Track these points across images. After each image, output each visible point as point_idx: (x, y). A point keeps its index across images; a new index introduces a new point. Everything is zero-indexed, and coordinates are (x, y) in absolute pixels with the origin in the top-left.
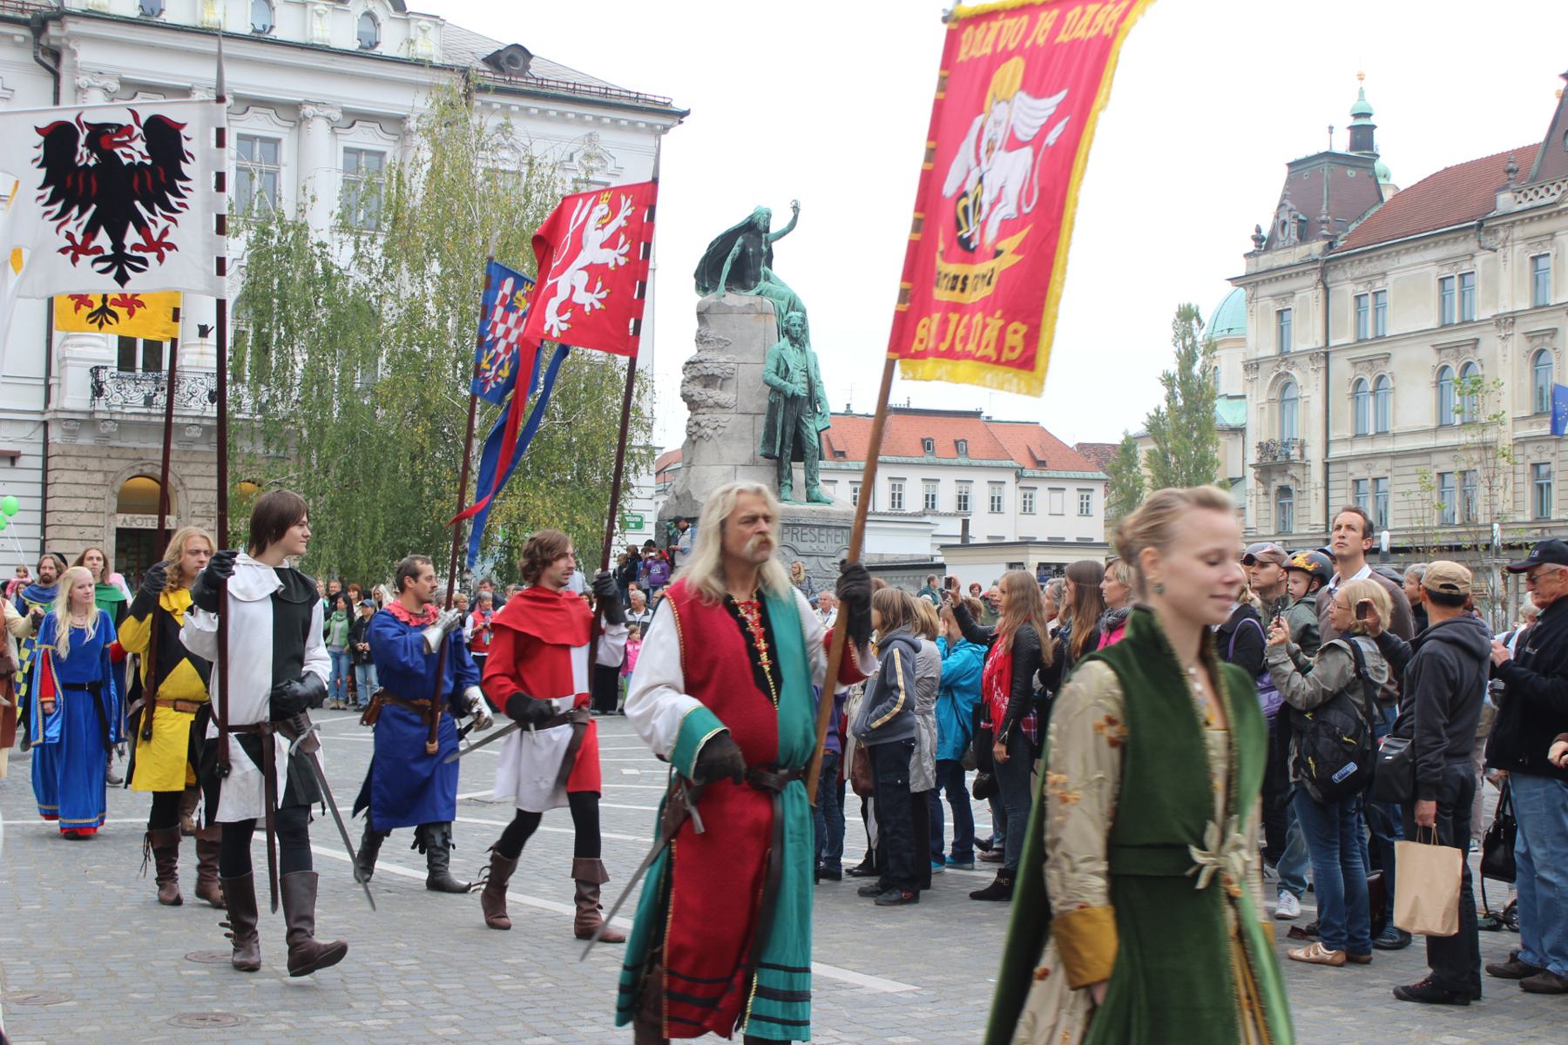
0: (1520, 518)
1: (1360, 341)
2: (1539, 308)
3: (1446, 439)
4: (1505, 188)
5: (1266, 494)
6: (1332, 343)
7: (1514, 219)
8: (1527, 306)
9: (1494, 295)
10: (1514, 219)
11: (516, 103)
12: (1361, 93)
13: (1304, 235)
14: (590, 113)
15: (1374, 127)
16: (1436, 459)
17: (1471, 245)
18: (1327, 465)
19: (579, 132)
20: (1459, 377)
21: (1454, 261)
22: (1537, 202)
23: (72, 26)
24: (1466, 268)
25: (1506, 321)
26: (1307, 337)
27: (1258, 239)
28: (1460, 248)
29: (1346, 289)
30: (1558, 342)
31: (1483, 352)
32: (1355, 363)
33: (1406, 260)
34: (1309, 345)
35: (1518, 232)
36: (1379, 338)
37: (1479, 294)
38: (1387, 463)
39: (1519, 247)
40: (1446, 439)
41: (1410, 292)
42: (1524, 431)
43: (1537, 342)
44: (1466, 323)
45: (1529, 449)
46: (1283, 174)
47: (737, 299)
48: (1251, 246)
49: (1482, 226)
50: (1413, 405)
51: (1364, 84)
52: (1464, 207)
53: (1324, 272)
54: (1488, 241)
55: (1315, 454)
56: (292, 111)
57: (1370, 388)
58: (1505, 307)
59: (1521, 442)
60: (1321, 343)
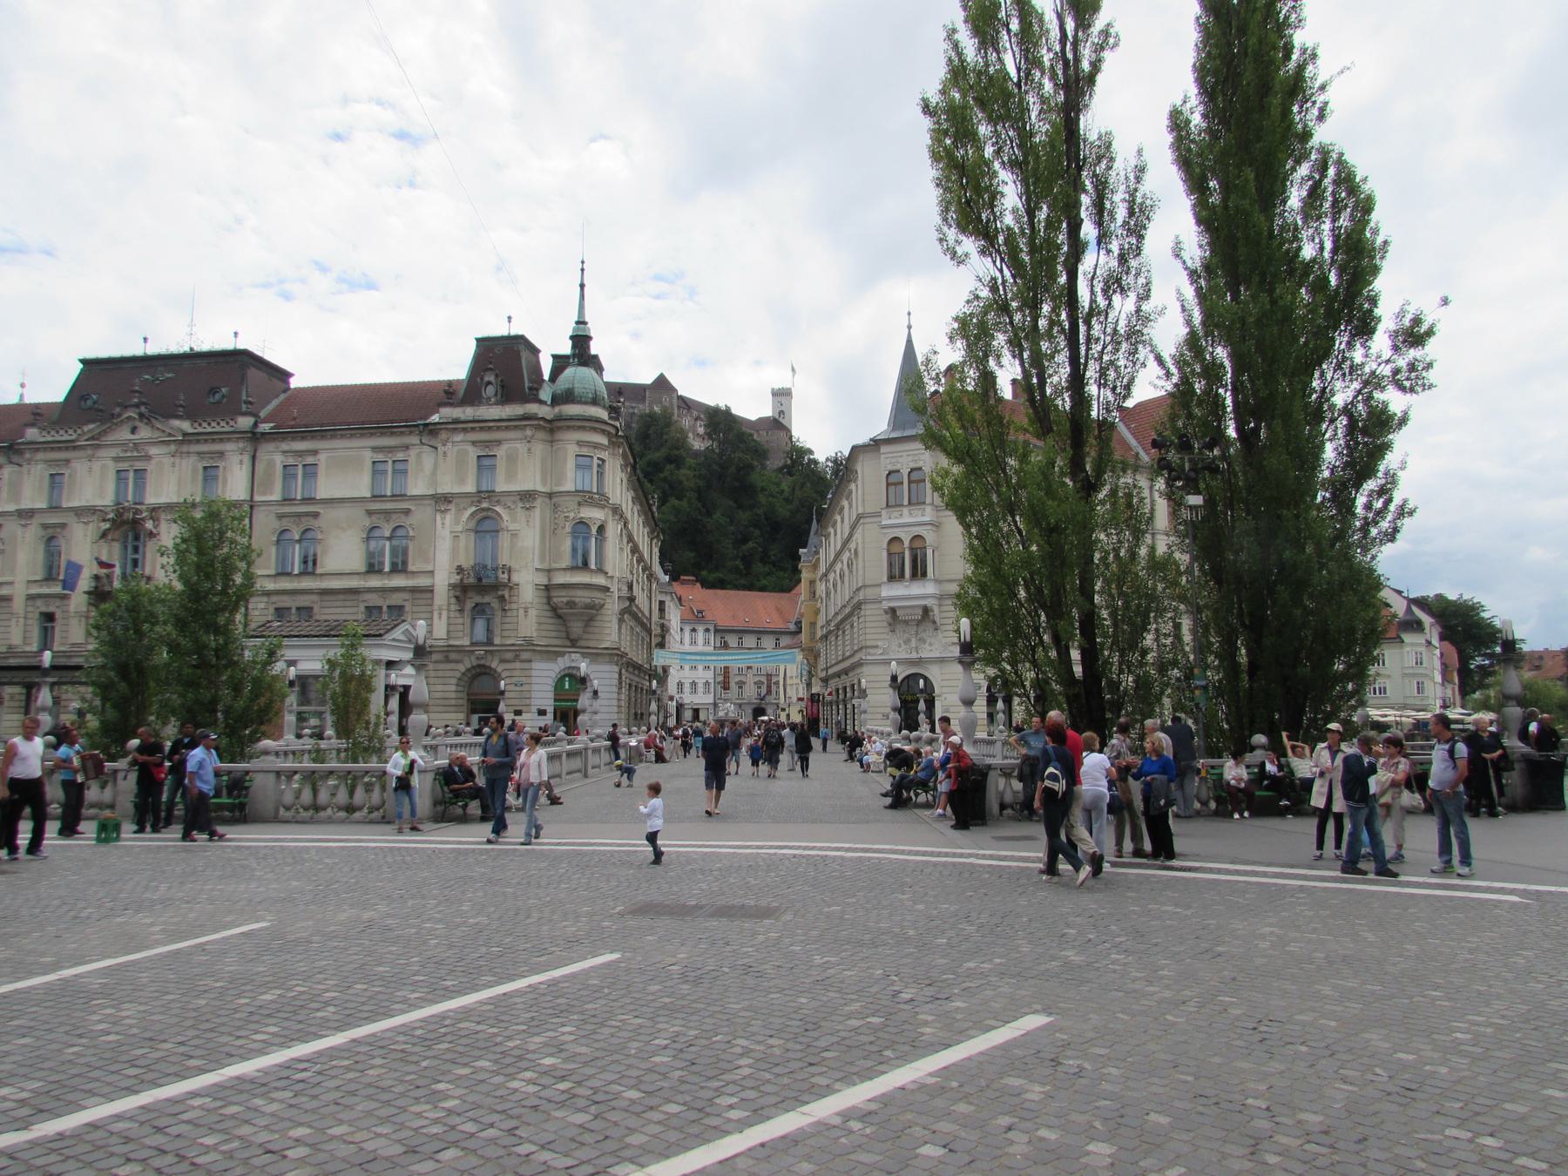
0: (28, 649)
2: (54, 508)
4: (32, 425)
7: (36, 446)
8: (42, 504)
10: (36, 446)
35: (40, 456)
39: (40, 467)
42: (35, 590)
43: (50, 531)
45: (39, 603)
54: (16, 459)
58: (26, 504)
59: (31, 598)
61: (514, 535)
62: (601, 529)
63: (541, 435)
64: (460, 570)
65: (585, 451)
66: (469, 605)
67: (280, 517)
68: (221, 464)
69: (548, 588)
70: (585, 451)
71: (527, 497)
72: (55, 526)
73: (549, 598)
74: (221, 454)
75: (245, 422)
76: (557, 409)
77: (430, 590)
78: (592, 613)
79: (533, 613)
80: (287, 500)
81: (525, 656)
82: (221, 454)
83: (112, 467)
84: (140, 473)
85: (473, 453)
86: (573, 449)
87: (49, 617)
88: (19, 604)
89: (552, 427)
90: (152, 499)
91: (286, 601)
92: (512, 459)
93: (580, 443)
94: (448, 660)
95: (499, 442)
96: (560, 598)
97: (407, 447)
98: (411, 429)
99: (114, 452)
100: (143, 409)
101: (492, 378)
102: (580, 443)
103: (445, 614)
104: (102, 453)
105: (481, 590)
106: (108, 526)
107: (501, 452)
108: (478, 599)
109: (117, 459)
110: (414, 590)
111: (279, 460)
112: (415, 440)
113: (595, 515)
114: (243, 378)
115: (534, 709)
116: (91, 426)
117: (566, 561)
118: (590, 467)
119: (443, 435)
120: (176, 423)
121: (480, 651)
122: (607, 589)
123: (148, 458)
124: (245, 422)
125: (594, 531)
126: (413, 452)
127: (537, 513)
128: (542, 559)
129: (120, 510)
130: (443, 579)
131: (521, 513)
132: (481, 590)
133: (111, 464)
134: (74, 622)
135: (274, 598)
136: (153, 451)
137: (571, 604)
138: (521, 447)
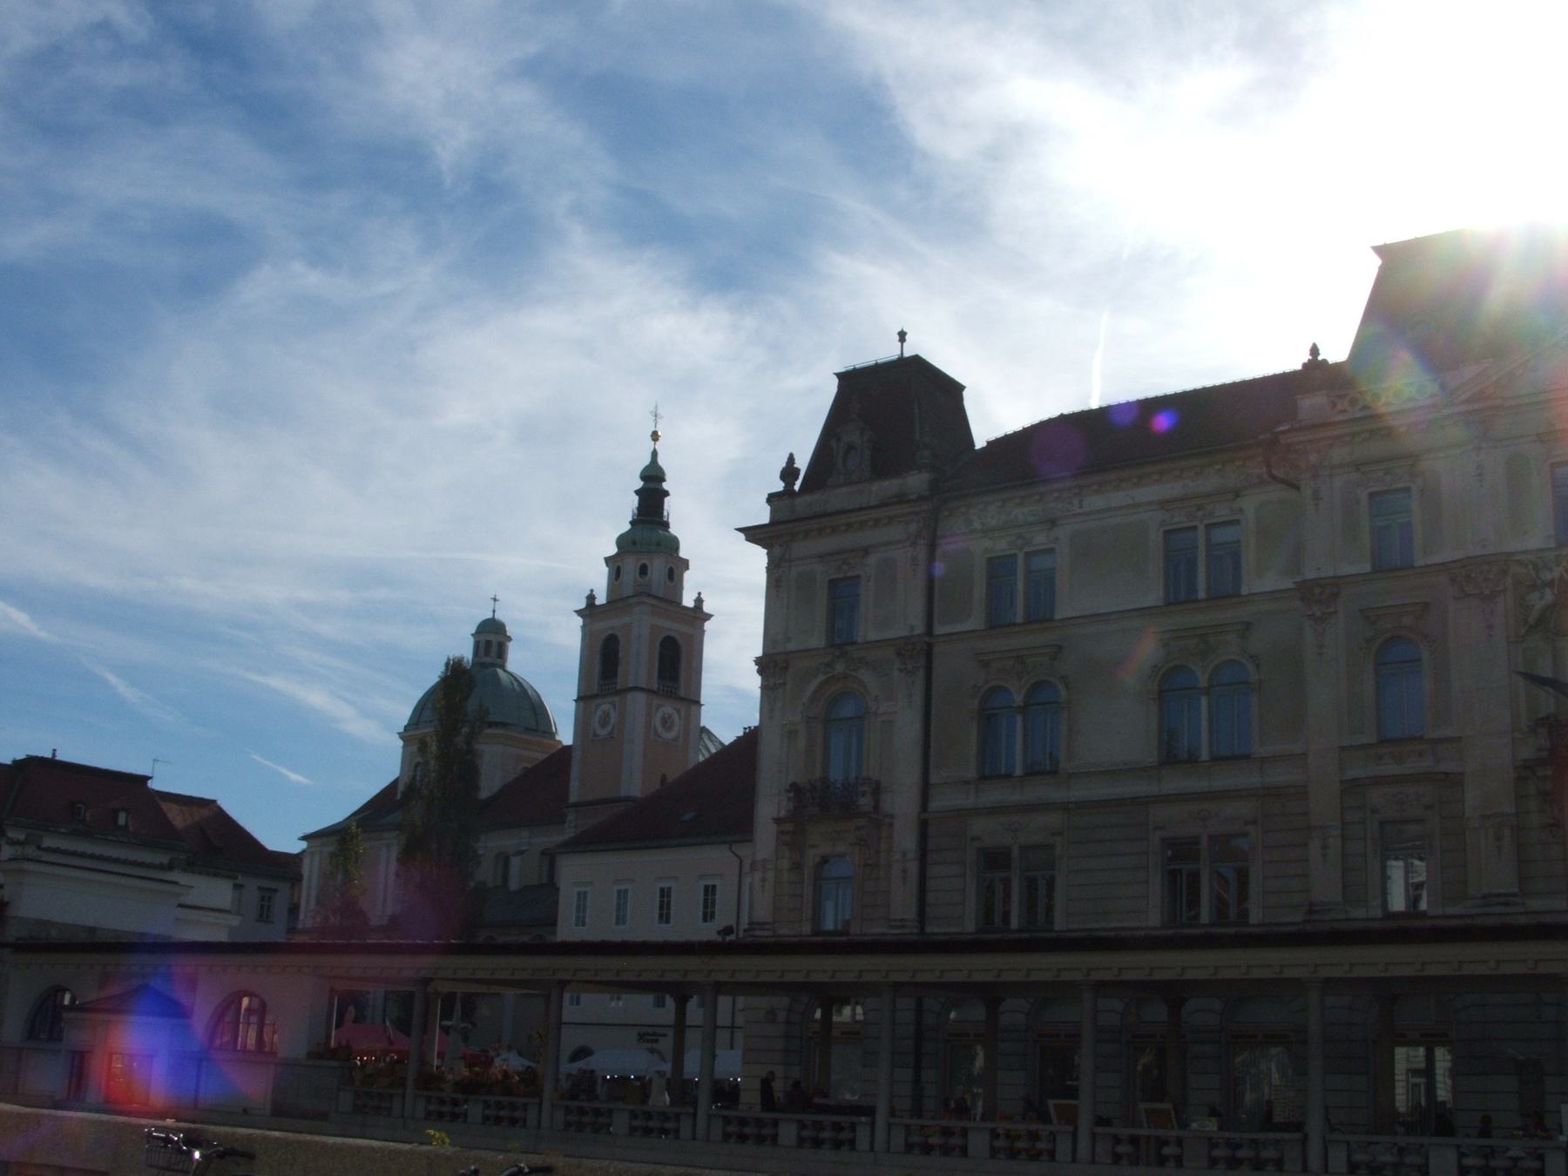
5: (797, 867)
6: (939, 629)
12: (655, 454)
13: (883, 466)
15: (666, 494)
18: (924, 825)
26: (891, 614)
27: (789, 473)
34: (897, 631)
40: (1175, 783)
46: (833, 386)
48: (779, 486)
51: (658, 446)
55: (902, 802)
57: (1018, 700)
60: (920, 629)
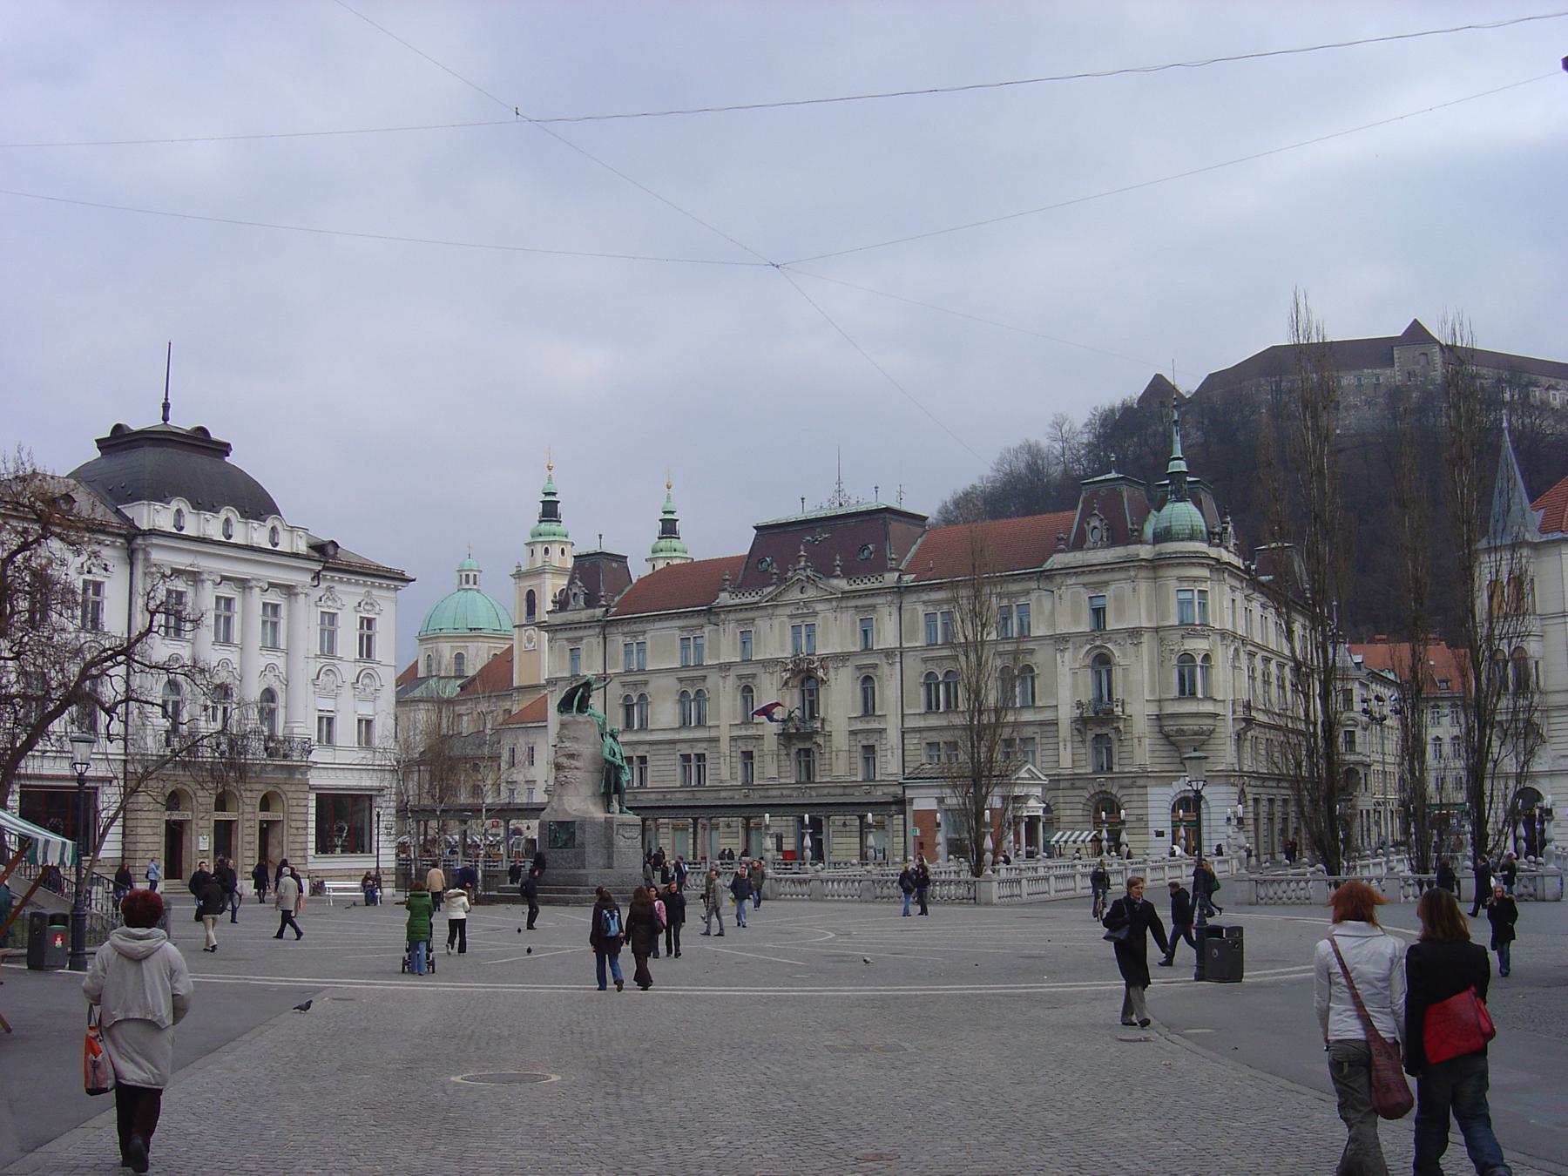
1: (628, 672)
2: (746, 661)
3: (684, 735)
9: (716, 651)
11: (337, 575)
14: (369, 580)
16: (679, 746)
17: (702, 620)
19: (362, 590)
20: (693, 701)
21: (691, 628)
22: (744, 600)
23: (155, 541)
24: (698, 633)
25: (725, 667)
28: (694, 622)
29: (618, 641)
30: (756, 682)
31: (709, 683)
32: (624, 685)
33: (658, 625)
35: (732, 616)
36: (642, 671)
37: (706, 651)
38: (647, 747)
40: (684, 735)
41: (662, 646)
42: (736, 733)
44: (699, 666)
45: (740, 743)
47: (581, 718)
49: (712, 613)
50: (664, 714)
52: (690, 593)
53: (604, 628)
54: (713, 619)
56: (243, 584)
59: (733, 739)
61: (1126, 670)
62: (1207, 658)
63: (1143, 574)
64: (1079, 705)
65: (1185, 586)
66: (1090, 736)
67: (925, 660)
68: (874, 616)
69: (1159, 717)
70: (1185, 586)
71: (1135, 633)
72: (748, 676)
73: (1161, 727)
74: (874, 607)
75: (891, 578)
76: (1158, 547)
77: (1055, 723)
78: (1203, 739)
79: (1146, 741)
80: (931, 645)
81: (1141, 782)
82: (874, 607)
83: (788, 624)
84: (811, 627)
85: (1085, 594)
86: (1173, 585)
87: (748, 755)
88: (724, 745)
89: (1156, 565)
90: (821, 651)
91: (934, 737)
92: (1119, 599)
93: (1180, 579)
94: (1073, 788)
95: (1107, 583)
96: (1170, 726)
97: (1027, 592)
98: (1029, 577)
99: (788, 611)
100: (809, 572)
101: (1097, 524)
102: (1180, 579)
103: (1069, 745)
104: (779, 611)
105: (1100, 722)
106: (786, 675)
107: (1109, 593)
108: (1098, 731)
109: (791, 617)
110: (1042, 724)
111: (920, 608)
112: (1033, 585)
113: (1198, 646)
114: (886, 534)
115: (1152, 831)
116: (770, 589)
117: (1175, 693)
118: (1191, 602)
119: (1058, 580)
120: (835, 582)
121: (1102, 778)
122: (1215, 715)
123: (815, 614)
124: (891, 578)
125: (1199, 661)
126: (1034, 596)
127: (1145, 648)
128: (1152, 691)
129: (797, 661)
130: (1066, 713)
131: (1130, 649)
132: (1100, 722)
133: (786, 620)
134: (768, 759)
135: (925, 734)
136: (819, 607)
137: (1181, 732)
138: (1127, 586)
